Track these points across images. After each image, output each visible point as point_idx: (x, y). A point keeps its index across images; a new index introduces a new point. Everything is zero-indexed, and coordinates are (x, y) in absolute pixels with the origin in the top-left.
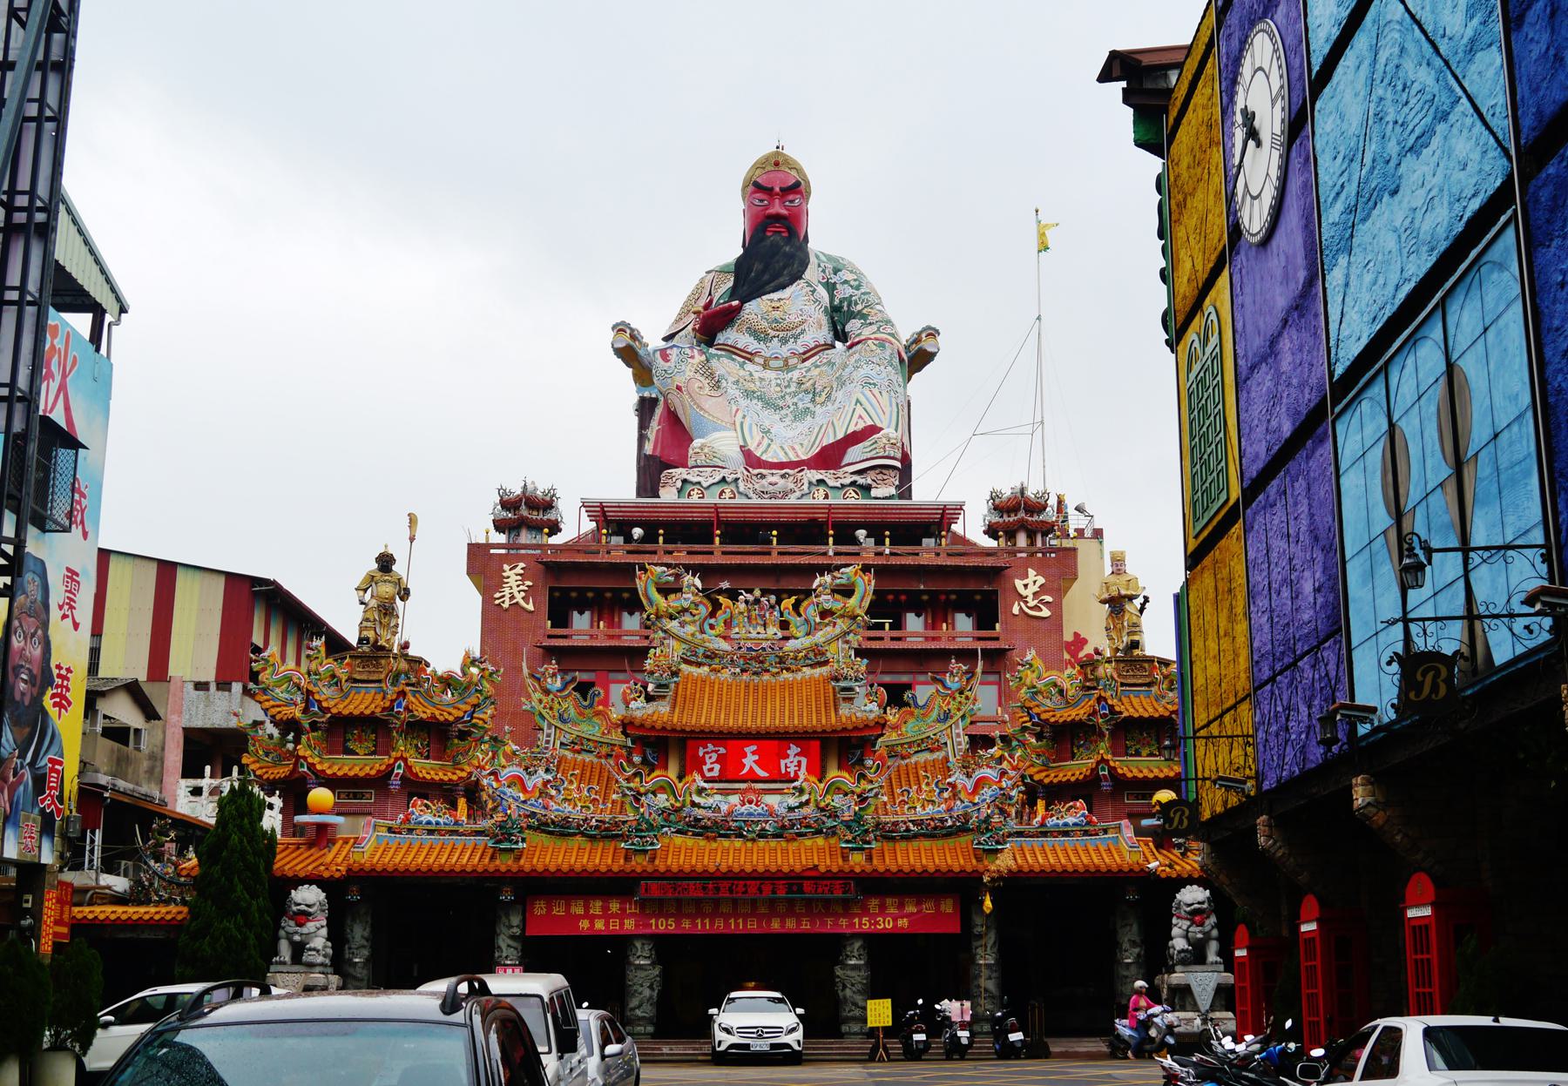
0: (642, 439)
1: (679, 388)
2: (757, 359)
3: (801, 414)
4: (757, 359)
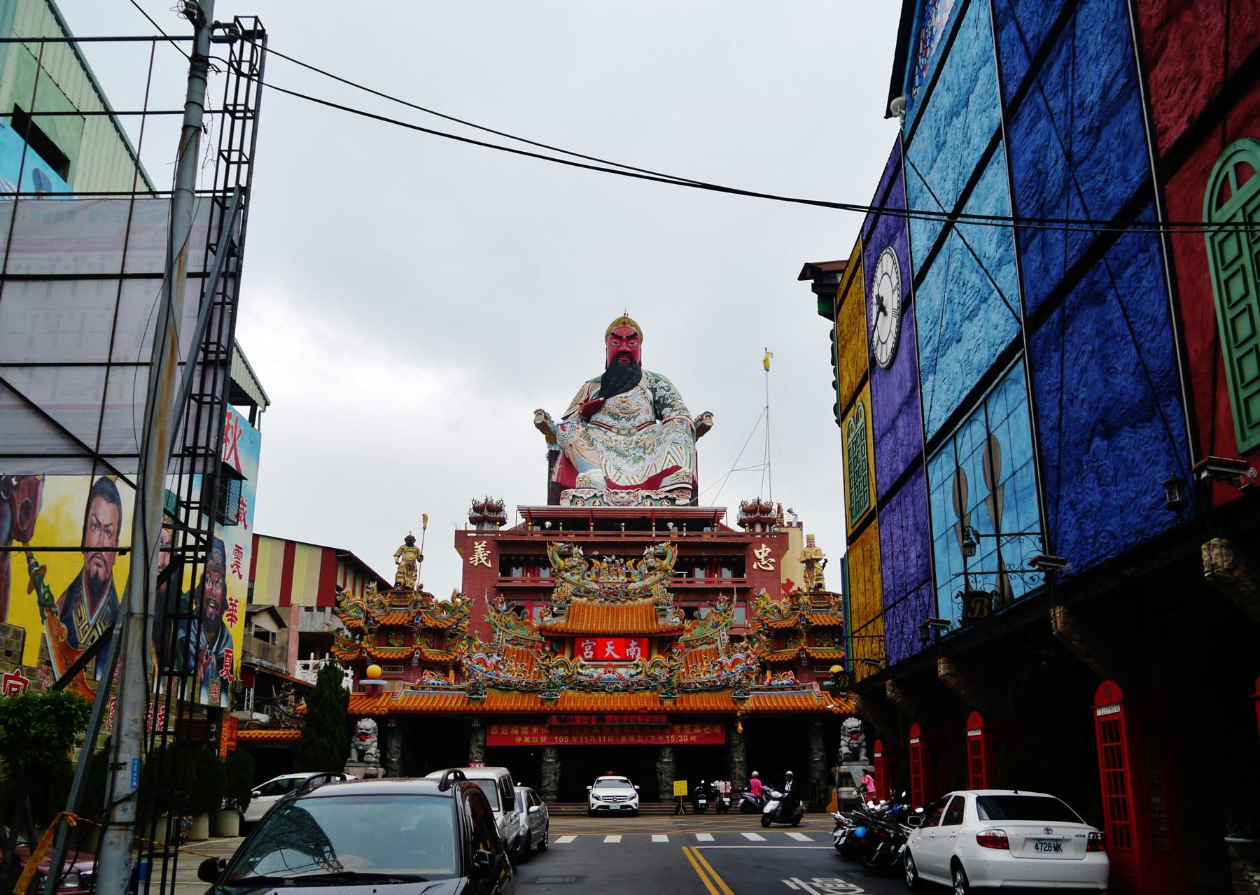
0: (551, 473)
3: (637, 460)
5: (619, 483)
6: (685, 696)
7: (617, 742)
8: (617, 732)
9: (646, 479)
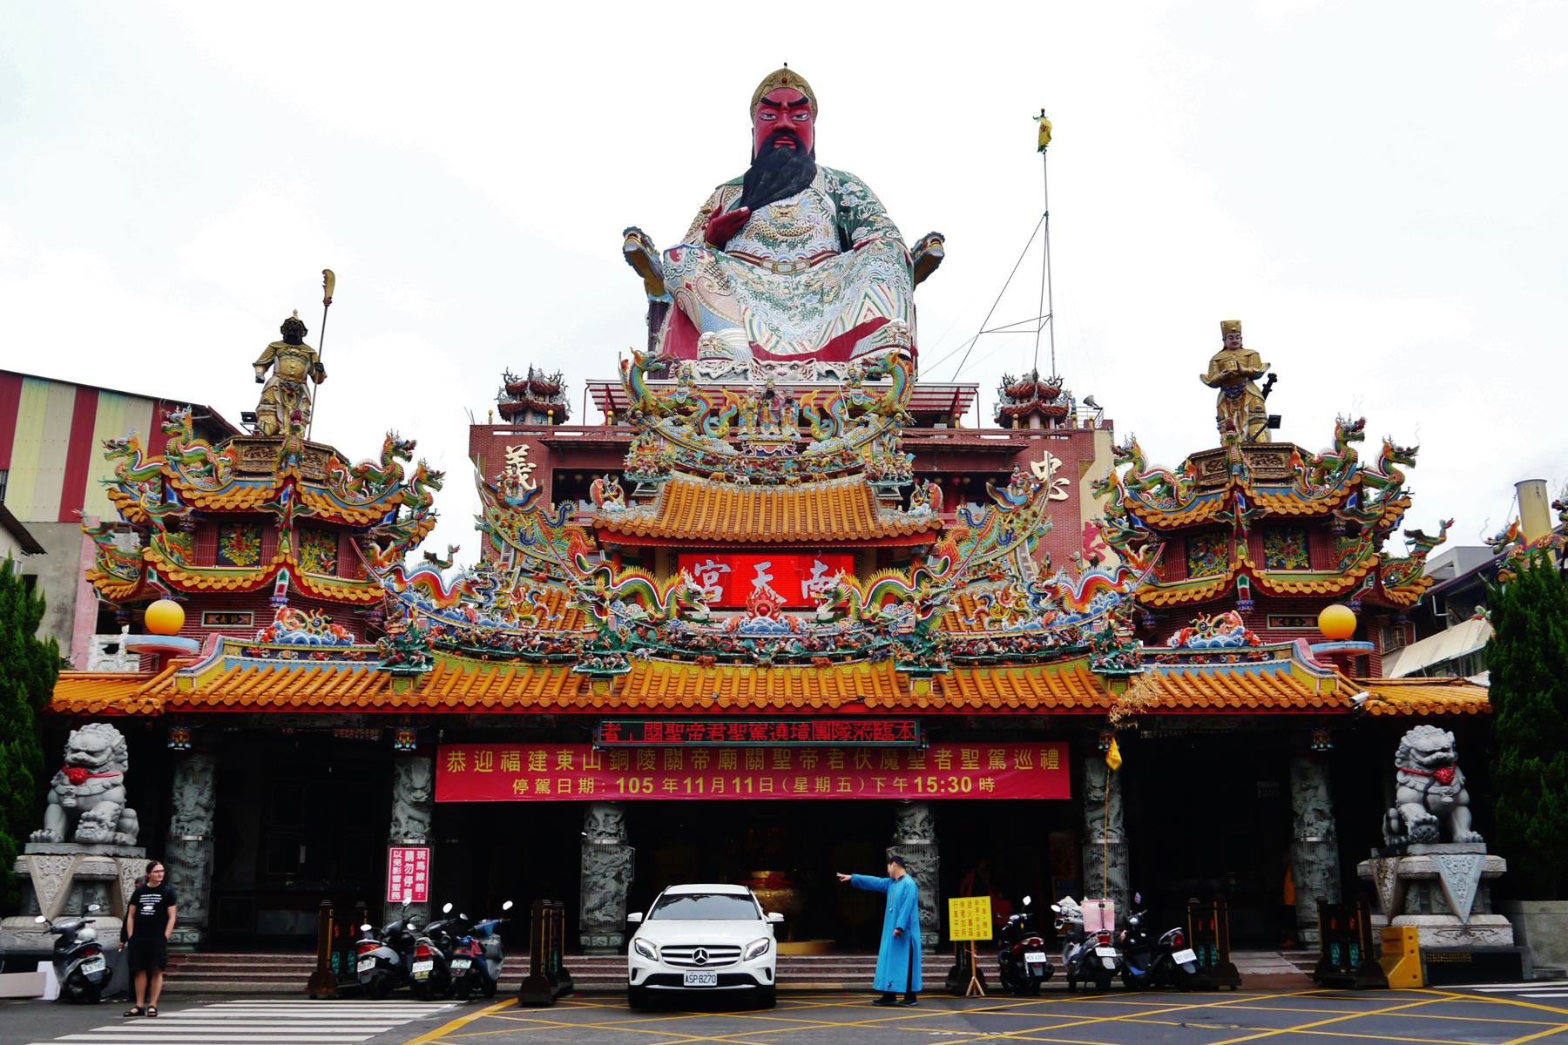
0: (652, 342)
1: (688, 286)
2: (765, 264)
4: (765, 264)
5: (778, 352)
6: (963, 674)
7: (784, 793)
8: (782, 765)
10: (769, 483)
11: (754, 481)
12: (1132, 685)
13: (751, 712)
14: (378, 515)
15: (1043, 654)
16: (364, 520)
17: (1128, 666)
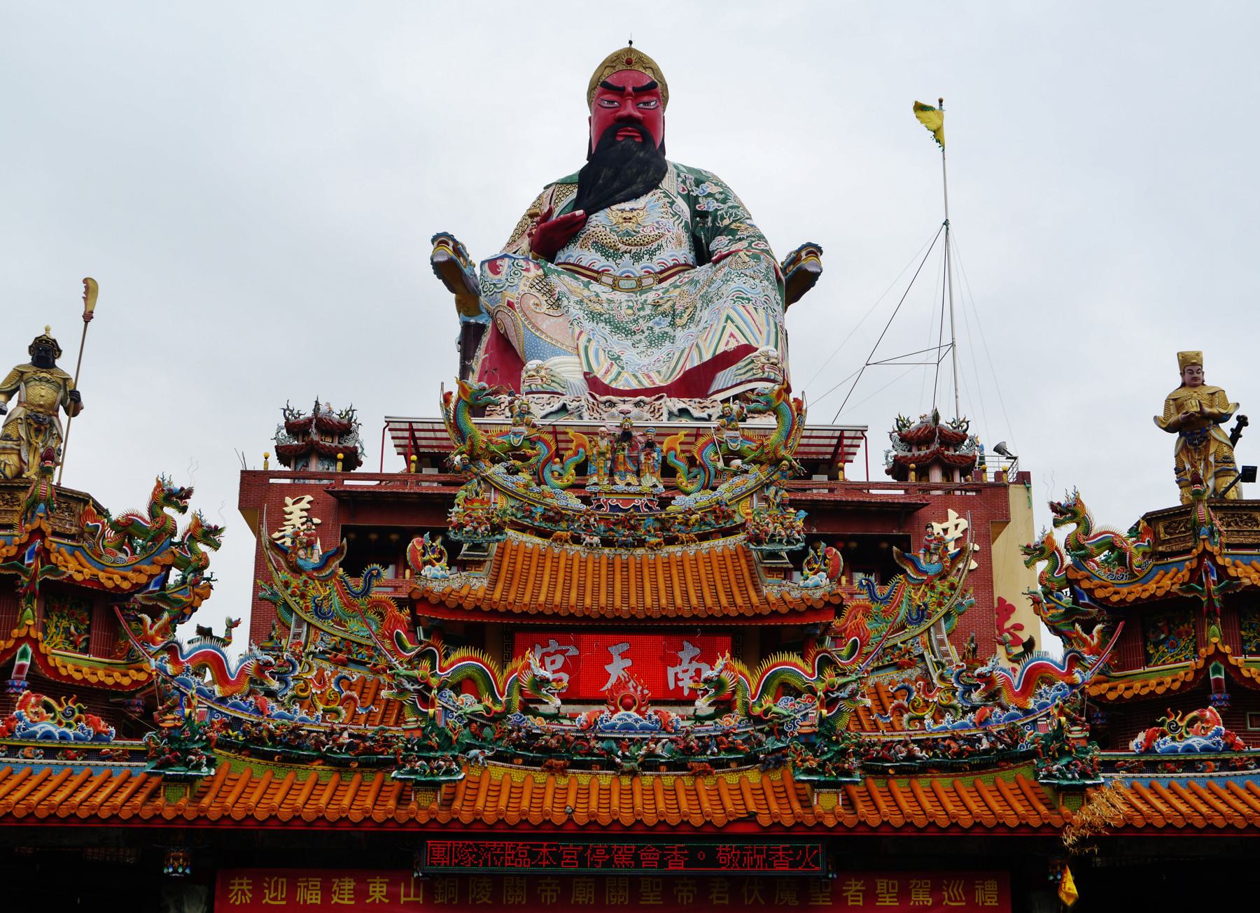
0: (465, 371)
1: (510, 304)
2: (604, 279)
3: (656, 341)
4: (604, 279)
5: (620, 385)
6: (876, 785)
9: (677, 375)
10: (624, 545)
11: (606, 543)
12: (1089, 801)
13: (616, 830)
14: (143, 579)
15: (976, 760)
16: (126, 585)
17: (1084, 775)
